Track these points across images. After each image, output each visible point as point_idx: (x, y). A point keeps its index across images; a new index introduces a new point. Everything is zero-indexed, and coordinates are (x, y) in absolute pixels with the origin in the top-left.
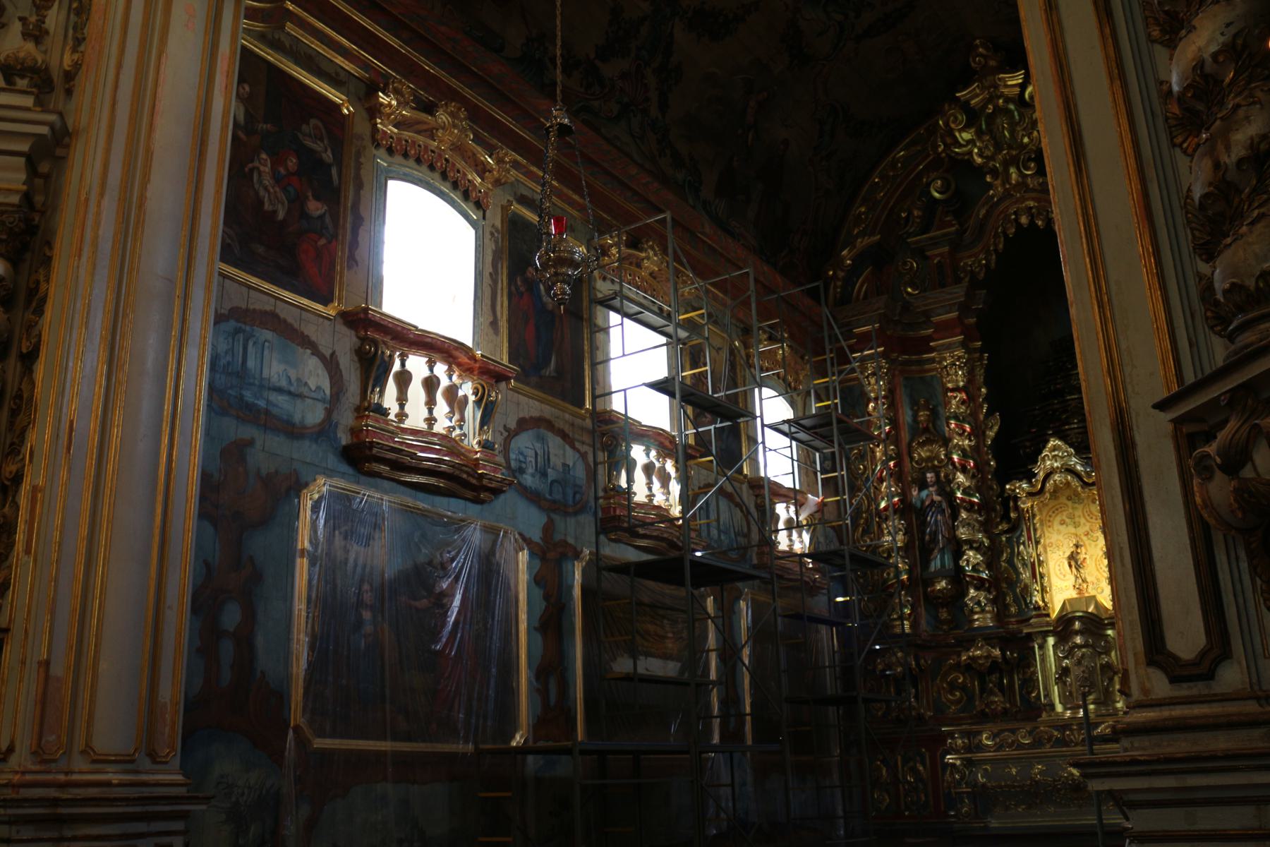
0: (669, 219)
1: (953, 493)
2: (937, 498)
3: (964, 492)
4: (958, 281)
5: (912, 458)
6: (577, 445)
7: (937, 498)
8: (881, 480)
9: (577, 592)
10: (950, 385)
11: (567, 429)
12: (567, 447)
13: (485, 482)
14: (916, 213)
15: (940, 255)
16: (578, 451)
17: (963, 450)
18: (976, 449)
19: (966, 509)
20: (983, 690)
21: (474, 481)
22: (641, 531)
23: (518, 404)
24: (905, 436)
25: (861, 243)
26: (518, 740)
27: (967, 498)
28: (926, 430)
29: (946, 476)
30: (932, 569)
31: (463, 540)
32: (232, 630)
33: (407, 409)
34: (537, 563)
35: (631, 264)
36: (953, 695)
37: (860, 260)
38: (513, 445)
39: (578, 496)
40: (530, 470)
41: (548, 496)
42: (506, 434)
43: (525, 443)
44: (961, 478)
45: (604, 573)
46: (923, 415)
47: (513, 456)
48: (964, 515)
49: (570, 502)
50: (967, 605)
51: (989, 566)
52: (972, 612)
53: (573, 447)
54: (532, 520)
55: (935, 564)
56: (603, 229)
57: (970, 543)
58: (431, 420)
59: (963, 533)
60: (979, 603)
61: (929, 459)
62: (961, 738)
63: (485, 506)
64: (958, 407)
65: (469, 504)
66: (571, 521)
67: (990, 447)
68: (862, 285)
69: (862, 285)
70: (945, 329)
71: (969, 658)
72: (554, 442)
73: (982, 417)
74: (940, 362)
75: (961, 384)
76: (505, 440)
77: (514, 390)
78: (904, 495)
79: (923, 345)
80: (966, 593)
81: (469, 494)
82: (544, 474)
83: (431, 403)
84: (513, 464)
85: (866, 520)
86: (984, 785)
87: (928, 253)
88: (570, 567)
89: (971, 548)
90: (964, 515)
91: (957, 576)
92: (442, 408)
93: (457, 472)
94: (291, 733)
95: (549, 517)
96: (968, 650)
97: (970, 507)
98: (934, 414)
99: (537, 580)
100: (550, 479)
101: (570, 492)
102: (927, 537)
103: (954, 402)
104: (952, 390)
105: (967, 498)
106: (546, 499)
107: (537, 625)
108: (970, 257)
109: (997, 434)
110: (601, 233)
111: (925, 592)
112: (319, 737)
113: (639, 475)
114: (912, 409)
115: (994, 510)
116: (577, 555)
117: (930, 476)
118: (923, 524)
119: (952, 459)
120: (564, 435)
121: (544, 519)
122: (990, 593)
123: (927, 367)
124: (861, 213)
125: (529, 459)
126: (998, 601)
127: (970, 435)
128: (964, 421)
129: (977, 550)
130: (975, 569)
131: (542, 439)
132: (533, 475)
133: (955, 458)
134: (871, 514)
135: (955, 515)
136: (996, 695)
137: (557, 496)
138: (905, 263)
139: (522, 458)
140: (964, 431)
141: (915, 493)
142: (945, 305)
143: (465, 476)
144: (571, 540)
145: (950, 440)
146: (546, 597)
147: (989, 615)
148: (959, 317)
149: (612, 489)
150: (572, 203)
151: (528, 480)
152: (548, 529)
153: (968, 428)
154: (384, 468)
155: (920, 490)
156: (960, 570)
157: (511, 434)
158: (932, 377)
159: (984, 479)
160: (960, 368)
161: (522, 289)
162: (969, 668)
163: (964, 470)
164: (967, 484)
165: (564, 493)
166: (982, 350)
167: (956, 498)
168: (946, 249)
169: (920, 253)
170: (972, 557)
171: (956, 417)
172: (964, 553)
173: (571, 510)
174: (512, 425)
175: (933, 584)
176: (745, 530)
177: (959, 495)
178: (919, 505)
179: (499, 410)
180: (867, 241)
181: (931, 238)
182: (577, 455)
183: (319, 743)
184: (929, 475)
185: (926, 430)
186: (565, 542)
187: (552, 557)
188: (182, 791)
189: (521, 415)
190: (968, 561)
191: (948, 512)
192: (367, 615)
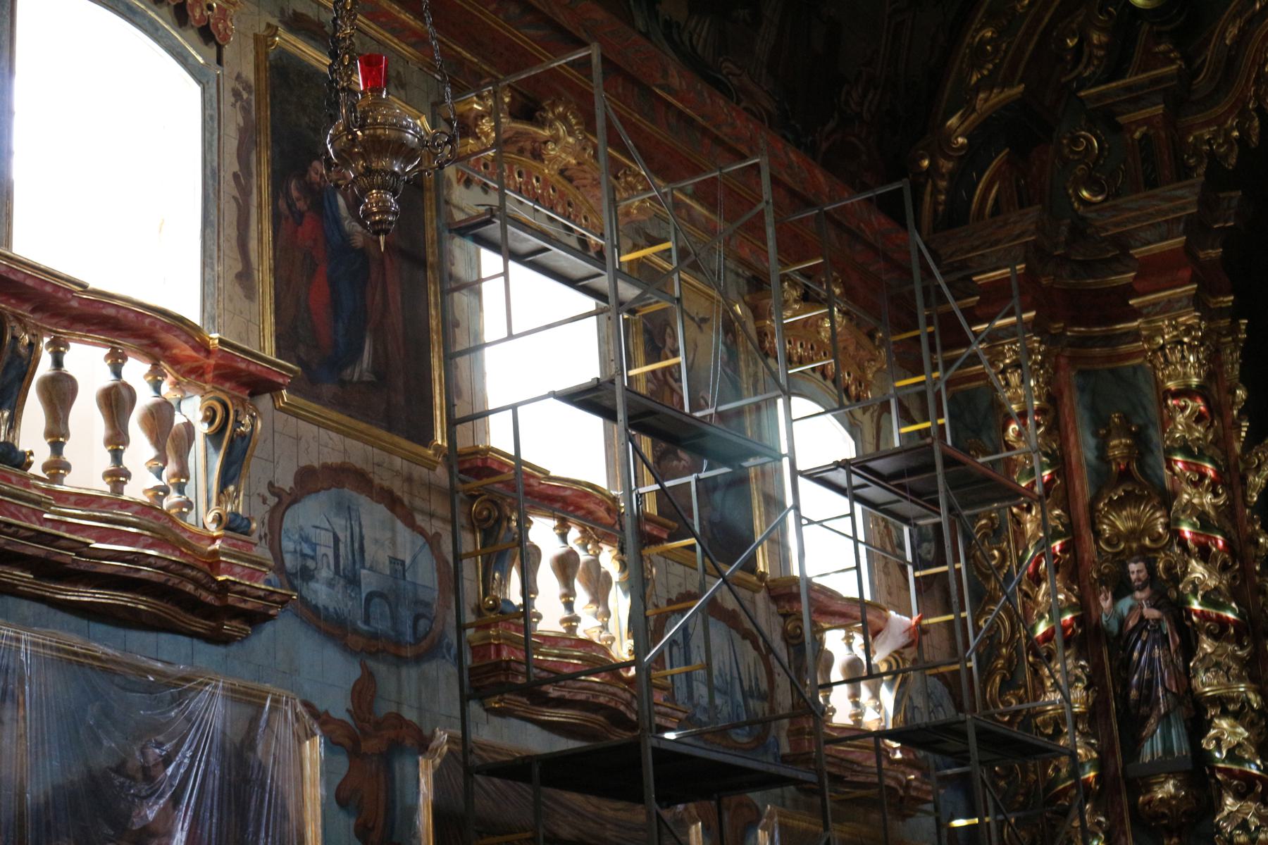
0: (596, 60)
1: (1183, 603)
2: (1152, 613)
3: (1206, 600)
4: (1183, 173)
5: (1098, 534)
6: (419, 519)
7: (1152, 613)
8: (1037, 579)
9: (425, 820)
10: (1171, 385)
11: (398, 488)
12: (399, 525)
13: (232, 599)
14: (1095, 38)
15: (1147, 121)
16: (422, 532)
17: (1202, 516)
18: (1229, 512)
19: (1210, 634)
21: (210, 598)
22: (553, 692)
23: (298, 439)
24: (1083, 488)
25: (986, 102)
27: (1213, 612)
28: (1125, 475)
29: (1169, 568)
30: (1147, 758)
31: (188, 719)
33: (68, 453)
34: (342, 763)
35: (521, 151)
37: (983, 138)
38: (288, 522)
39: (423, 623)
40: (325, 573)
41: (360, 624)
42: (273, 501)
43: (313, 518)
45: (479, 778)
46: (1118, 446)
47: (288, 545)
48: (1207, 646)
49: (409, 637)
50: (1220, 830)
53: (411, 524)
54: (330, 675)
55: (1152, 748)
56: (463, 80)
57: (1222, 703)
58: (118, 476)
59: (1206, 683)
60: (1244, 825)
61: (1133, 534)
63: (234, 648)
64: (1189, 428)
65: (200, 645)
66: (410, 674)
68: (988, 189)
69: (988, 189)
70: (1157, 271)
72: (373, 514)
73: (1238, 447)
74: (1149, 339)
75: (1195, 381)
76: (273, 510)
77: (288, 410)
78: (1084, 609)
79: (1115, 305)
81: (200, 625)
82: (353, 581)
83: (117, 440)
84: (289, 561)
85: (1009, 660)
87: (1122, 119)
88: (409, 769)
89: (1225, 713)
90: (1207, 646)
91: (1199, 774)
92: (140, 450)
93: (174, 581)
95: (364, 667)
97: (1220, 631)
98: (1141, 444)
99: (343, 798)
100: (365, 591)
101: (406, 615)
102: (1134, 693)
103: (1180, 418)
104: (1177, 394)
105: (1213, 612)
106: (356, 631)
108: (1207, 124)
110: (459, 91)
111: (1134, 807)
113: (547, 579)
114: (1095, 434)
116: (423, 745)
117: (1135, 569)
118: (1125, 666)
119: (1178, 533)
120: (391, 501)
121: (355, 672)
123: (1124, 348)
124: (983, 42)
125: (321, 550)
127: (1214, 483)
128: (1201, 455)
129: (1237, 716)
130: (1232, 755)
131: (347, 510)
132: (330, 584)
133: (1186, 530)
134: (1017, 649)
135: (1189, 648)
138: (1075, 141)
139: (307, 551)
140: (1203, 476)
141: (1106, 604)
142: (1158, 222)
143: (190, 588)
144: (410, 715)
145: (1175, 495)
148: (1188, 249)
149: (492, 609)
150: (400, 31)
151: (321, 593)
152: (363, 693)
153: (1209, 469)
154: (22, 576)
155: (1117, 597)
156: (1202, 758)
157: (283, 501)
159: (1245, 572)
160: (1191, 348)
161: (301, 205)
163: (1205, 555)
164: (1212, 583)
165: (395, 618)
166: (1235, 313)
167: (1190, 612)
168: (1159, 109)
169: (1106, 119)
170: (1227, 732)
171: (1186, 450)
172: (1209, 725)
173: (409, 652)
174: (286, 482)
175: (1148, 789)
176: (764, 686)
177: (1196, 605)
178: (1114, 627)
179: (259, 451)
180: (998, 97)
181: (1128, 89)
182: (420, 541)
184: (1133, 567)
185: (1125, 475)
186: (399, 717)
187: (370, 747)
189: (304, 462)
190: (1218, 740)
191: (1174, 641)
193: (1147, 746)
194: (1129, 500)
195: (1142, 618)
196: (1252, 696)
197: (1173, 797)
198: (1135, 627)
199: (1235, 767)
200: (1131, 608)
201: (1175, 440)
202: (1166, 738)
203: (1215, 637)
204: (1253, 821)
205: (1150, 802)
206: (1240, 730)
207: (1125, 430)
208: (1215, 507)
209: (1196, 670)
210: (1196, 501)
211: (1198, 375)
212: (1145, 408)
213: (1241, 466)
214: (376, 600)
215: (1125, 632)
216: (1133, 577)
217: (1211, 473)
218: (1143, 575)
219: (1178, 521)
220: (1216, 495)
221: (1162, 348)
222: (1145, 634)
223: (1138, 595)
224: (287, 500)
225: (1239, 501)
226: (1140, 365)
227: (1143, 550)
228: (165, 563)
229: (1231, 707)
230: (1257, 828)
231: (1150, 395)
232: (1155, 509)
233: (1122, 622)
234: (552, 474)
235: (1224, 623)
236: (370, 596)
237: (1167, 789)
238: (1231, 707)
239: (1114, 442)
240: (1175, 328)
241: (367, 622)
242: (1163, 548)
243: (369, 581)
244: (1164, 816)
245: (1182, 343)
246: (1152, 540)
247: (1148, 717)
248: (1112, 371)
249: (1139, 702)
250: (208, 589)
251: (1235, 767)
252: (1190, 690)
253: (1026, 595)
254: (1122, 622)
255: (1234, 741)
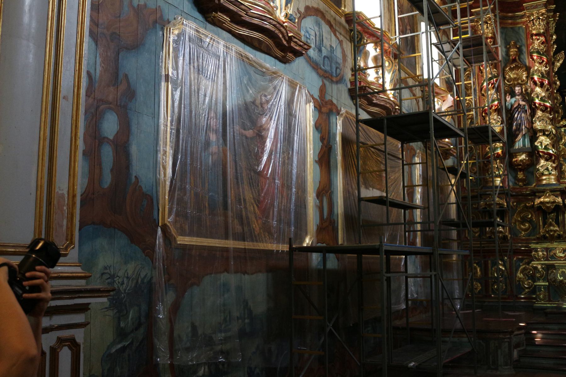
1: (533, 100)
2: (522, 103)
3: (542, 99)
6: (337, 33)
7: (522, 103)
9: (338, 138)
10: (534, 32)
11: (333, 22)
12: (332, 34)
16: (338, 39)
17: (542, 73)
18: (548, 73)
19: (541, 110)
20: (545, 223)
26: (307, 242)
28: (514, 60)
30: (517, 146)
31: (275, 88)
32: (111, 138)
36: (524, 225)
38: (302, 24)
39: (338, 70)
43: (309, 23)
44: (538, 89)
45: (360, 123)
46: (513, 51)
48: (539, 113)
49: (334, 75)
50: (538, 170)
51: (553, 147)
52: (543, 174)
53: (335, 35)
55: (519, 144)
57: (543, 132)
59: (538, 125)
60: (547, 169)
61: (515, 79)
62: (542, 251)
63: (287, 65)
64: (539, 46)
66: (335, 87)
67: (556, 73)
71: (541, 202)
72: (325, 28)
74: (529, 17)
75: (542, 31)
80: (538, 162)
81: (279, 53)
82: (320, 50)
86: (561, 281)
88: (334, 120)
89: (544, 135)
90: (539, 113)
91: (534, 154)
94: (159, 229)
95: (323, 81)
96: (540, 197)
97: (545, 109)
99: (317, 127)
100: (324, 54)
101: (334, 66)
102: (514, 127)
104: (536, 35)
106: (321, 68)
107: (317, 159)
109: (561, 65)
112: (181, 235)
114: (506, 47)
115: (558, 112)
116: (338, 113)
117: (517, 89)
119: (533, 78)
120: (331, 26)
121: (321, 83)
122: (554, 163)
123: (519, 21)
125: (312, 37)
126: (558, 168)
127: (546, 64)
128: (543, 54)
129: (547, 136)
130: (546, 148)
131: (319, 25)
132: (314, 50)
133: (536, 78)
135: (533, 114)
136: (554, 226)
137: (327, 68)
139: (308, 36)
140: (543, 61)
143: (281, 36)
144: (335, 101)
146: (322, 139)
147: (553, 177)
157: (303, 17)
158: (519, 28)
159: (552, 92)
160: (543, 20)
162: (542, 210)
163: (542, 85)
164: (543, 94)
165: (331, 66)
166: (555, 11)
167: (535, 104)
170: (543, 141)
171: (538, 52)
172: (537, 138)
173: (334, 79)
177: (537, 101)
178: (510, 107)
182: (338, 42)
183: (182, 240)
185: (514, 60)
186: (332, 101)
188: (81, 284)
189: (307, 4)
190: (541, 143)
191: (529, 112)
192: (213, 137)
193: (517, 144)
194: (517, 68)
195: (519, 104)
196: (553, 130)
197: (524, 159)
198: (516, 107)
199: (545, 151)
200: (515, 101)
201: (535, 49)
202: (524, 141)
203: (543, 111)
204: (550, 168)
205: (516, 161)
206: (548, 140)
207: (515, 46)
208: (546, 71)
209: (535, 121)
210: (540, 69)
211: (543, 29)
212: (521, 40)
213: (553, 59)
214: (326, 59)
215: (513, 109)
216: (517, 92)
217: (545, 60)
218: (520, 91)
219: (533, 74)
220: (546, 67)
221: (533, 20)
222: (520, 110)
223: (517, 97)
224: (302, 16)
225: (551, 70)
226: (521, 27)
227: (518, 84)
228: (276, 23)
229: (547, 133)
230: (552, 170)
231: (523, 36)
232: (523, 71)
233: (512, 106)
234: (376, 26)
235: (546, 107)
236: (325, 57)
237: (523, 157)
238: (547, 133)
239: (512, 50)
240: (538, 14)
241: (324, 66)
242: (524, 84)
243: (325, 52)
244: (520, 165)
245: (539, 19)
246: (522, 81)
247: (518, 135)
248: (512, 28)
249: (516, 130)
250: (285, 39)
251: (545, 151)
252: (532, 127)
253: (483, 95)
254: (512, 106)
255: (546, 143)
